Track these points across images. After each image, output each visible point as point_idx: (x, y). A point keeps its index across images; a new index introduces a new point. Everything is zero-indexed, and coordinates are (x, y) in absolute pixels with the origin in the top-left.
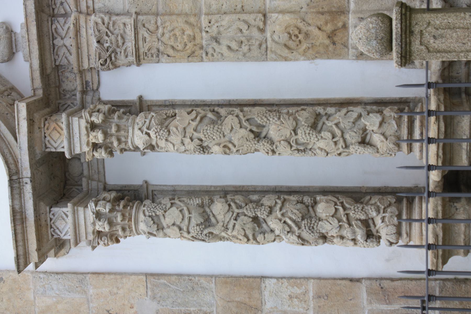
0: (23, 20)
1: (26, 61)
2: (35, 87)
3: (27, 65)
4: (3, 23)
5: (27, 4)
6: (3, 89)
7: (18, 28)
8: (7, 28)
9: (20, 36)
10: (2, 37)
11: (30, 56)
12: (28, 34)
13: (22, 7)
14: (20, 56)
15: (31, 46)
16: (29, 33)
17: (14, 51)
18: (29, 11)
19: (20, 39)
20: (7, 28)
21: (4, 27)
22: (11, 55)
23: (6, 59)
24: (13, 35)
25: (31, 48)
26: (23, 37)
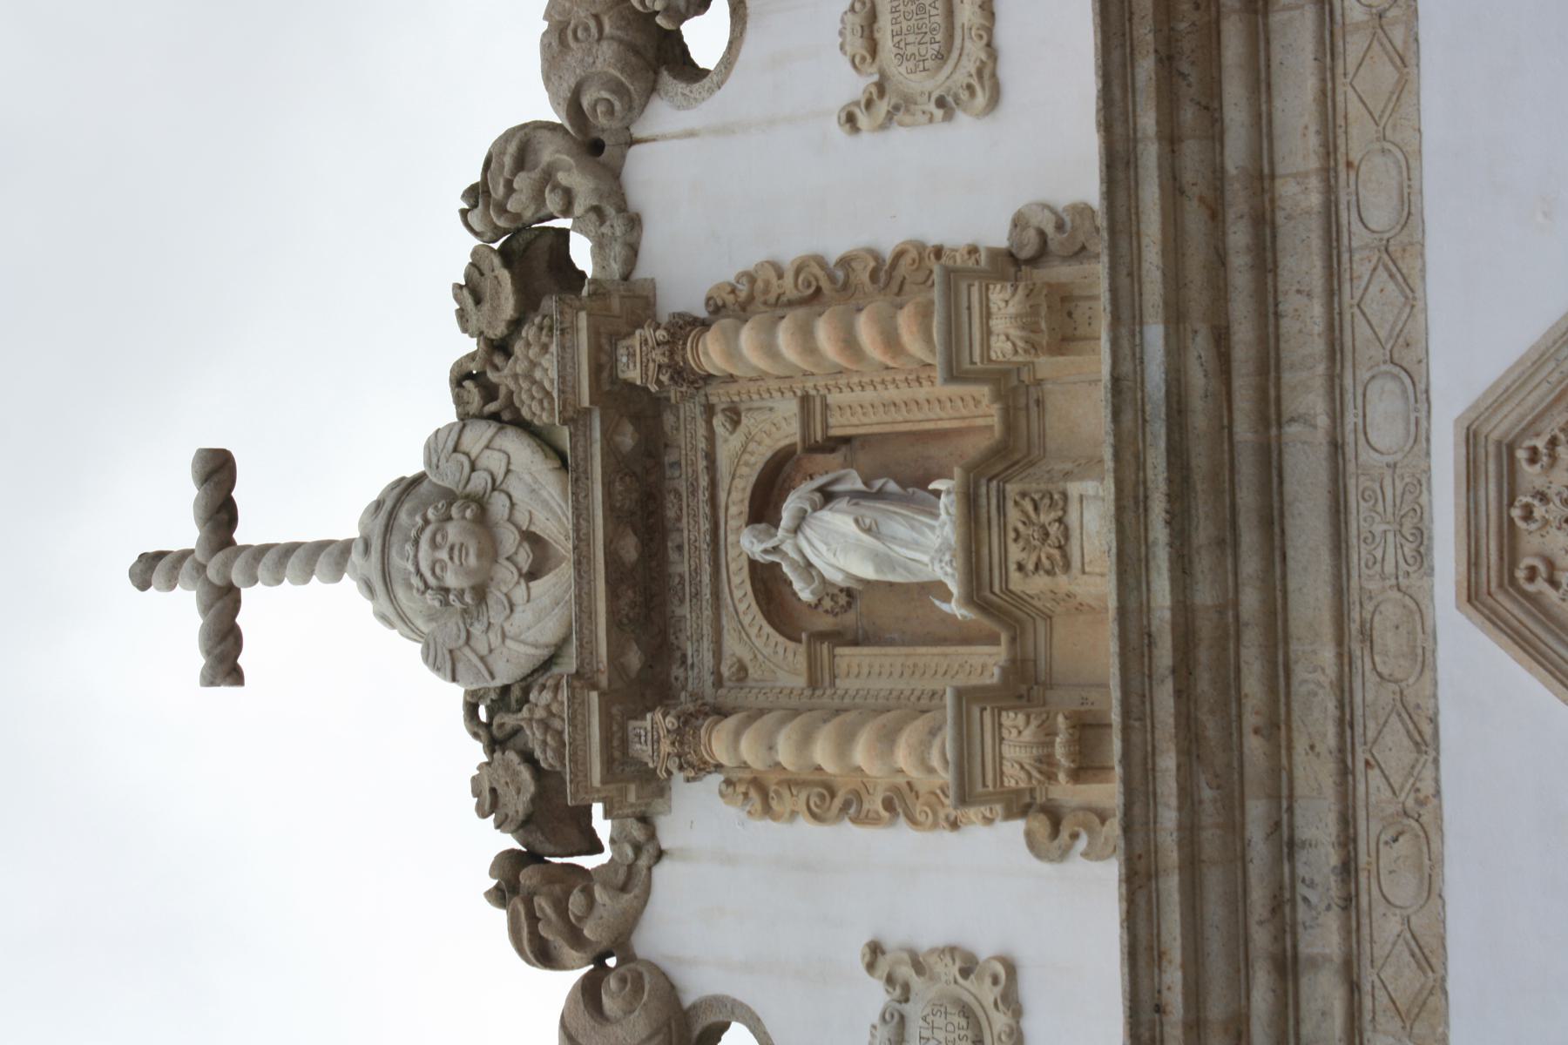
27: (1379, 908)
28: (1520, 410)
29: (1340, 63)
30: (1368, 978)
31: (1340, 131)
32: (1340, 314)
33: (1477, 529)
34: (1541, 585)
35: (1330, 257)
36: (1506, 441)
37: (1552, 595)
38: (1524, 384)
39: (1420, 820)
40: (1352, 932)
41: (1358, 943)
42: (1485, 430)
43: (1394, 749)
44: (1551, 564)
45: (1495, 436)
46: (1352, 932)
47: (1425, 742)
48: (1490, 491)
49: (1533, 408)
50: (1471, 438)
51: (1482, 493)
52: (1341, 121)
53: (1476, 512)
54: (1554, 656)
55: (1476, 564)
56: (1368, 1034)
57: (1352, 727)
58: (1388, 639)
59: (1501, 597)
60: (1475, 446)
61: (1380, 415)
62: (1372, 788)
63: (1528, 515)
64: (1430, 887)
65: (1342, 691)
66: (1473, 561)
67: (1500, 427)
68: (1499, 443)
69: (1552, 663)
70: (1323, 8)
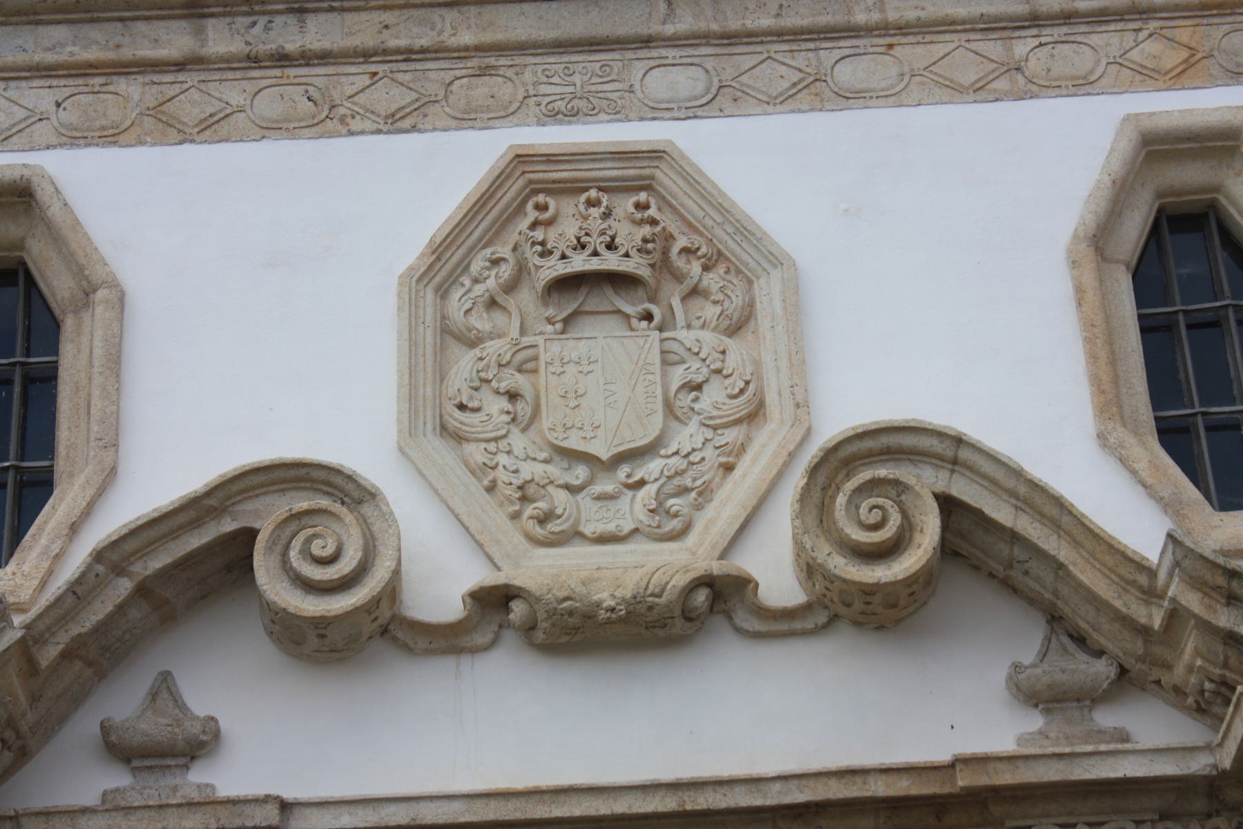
0: (225, 790)
1: (105, 794)
2: (24, 821)
3: (91, 798)
4: (217, 735)
5: (269, 807)
6: (24, 728)
7: (198, 775)
8: (202, 745)
9: (178, 781)
10: (177, 730)
11: (117, 809)
12: (180, 805)
13: (260, 790)
14: (119, 778)
15: (146, 814)
16: (186, 810)
17: (136, 763)
18: (248, 809)
19: (170, 780)
20: (202, 745)
21: (204, 738)
22: (121, 750)
23: (113, 738)
24: (181, 761)
25: (139, 814)
26: (175, 789)
27: (251, 87)
28: (681, 194)
29: (978, 36)
30: (191, 78)
31: (919, 38)
32: (762, 42)
33: (581, 161)
34: (532, 215)
35: (811, 32)
36: (654, 184)
37: (524, 224)
38: (703, 196)
39: (328, 119)
40: (228, 63)
41: (220, 69)
42: (663, 166)
43: (389, 96)
44: (550, 223)
45: (658, 174)
46: (228, 63)
47: (394, 122)
48: (612, 171)
49: (682, 205)
50: (656, 154)
51: (609, 165)
52: (928, 38)
53: (592, 160)
54: (472, 227)
55: (549, 161)
56: (140, 78)
57: (405, 60)
58: (482, 89)
59: (521, 182)
60: (650, 158)
61: (676, 79)
62: (353, 78)
63: (591, 203)
64: (270, 129)
65: (436, 51)
66: (551, 159)
67: (665, 177)
68: (652, 178)
69: (466, 225)
70: (1026, 20)
